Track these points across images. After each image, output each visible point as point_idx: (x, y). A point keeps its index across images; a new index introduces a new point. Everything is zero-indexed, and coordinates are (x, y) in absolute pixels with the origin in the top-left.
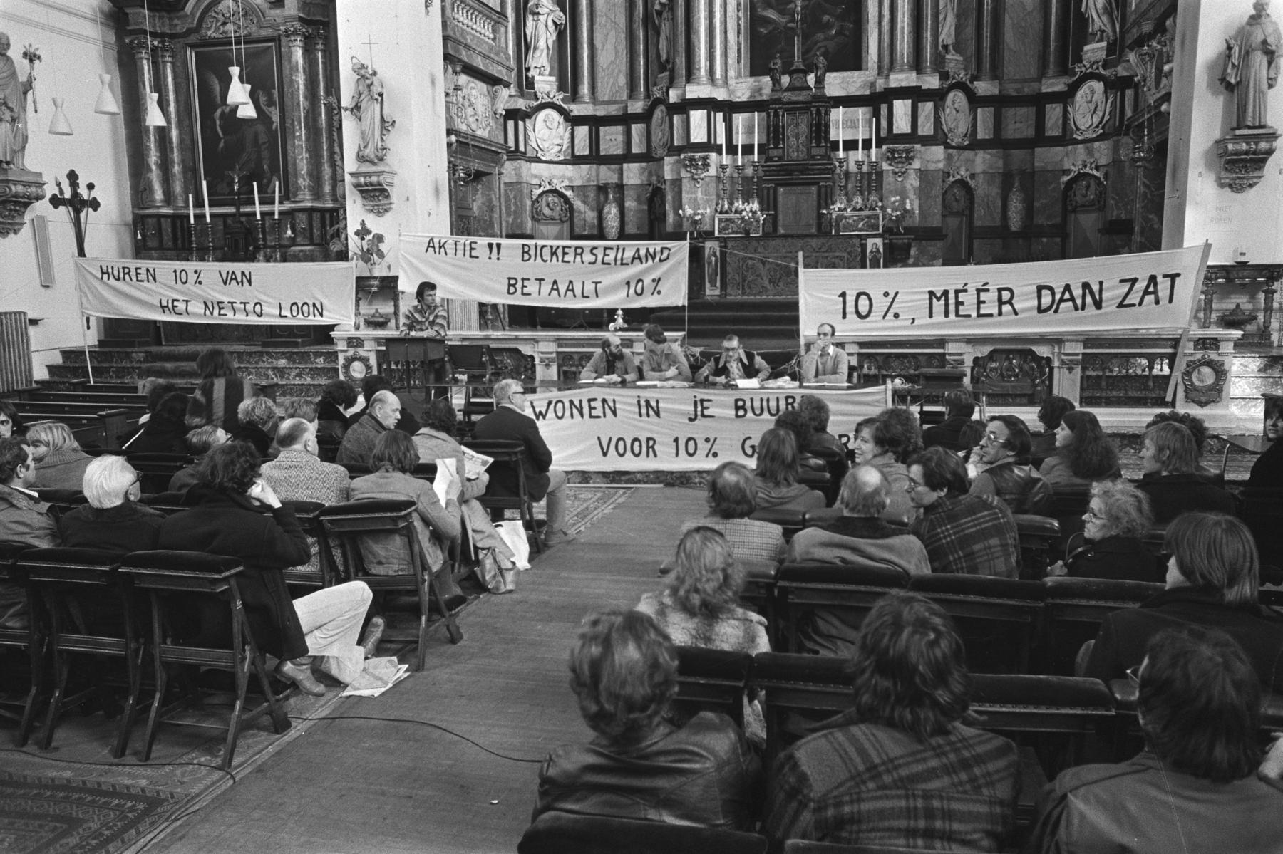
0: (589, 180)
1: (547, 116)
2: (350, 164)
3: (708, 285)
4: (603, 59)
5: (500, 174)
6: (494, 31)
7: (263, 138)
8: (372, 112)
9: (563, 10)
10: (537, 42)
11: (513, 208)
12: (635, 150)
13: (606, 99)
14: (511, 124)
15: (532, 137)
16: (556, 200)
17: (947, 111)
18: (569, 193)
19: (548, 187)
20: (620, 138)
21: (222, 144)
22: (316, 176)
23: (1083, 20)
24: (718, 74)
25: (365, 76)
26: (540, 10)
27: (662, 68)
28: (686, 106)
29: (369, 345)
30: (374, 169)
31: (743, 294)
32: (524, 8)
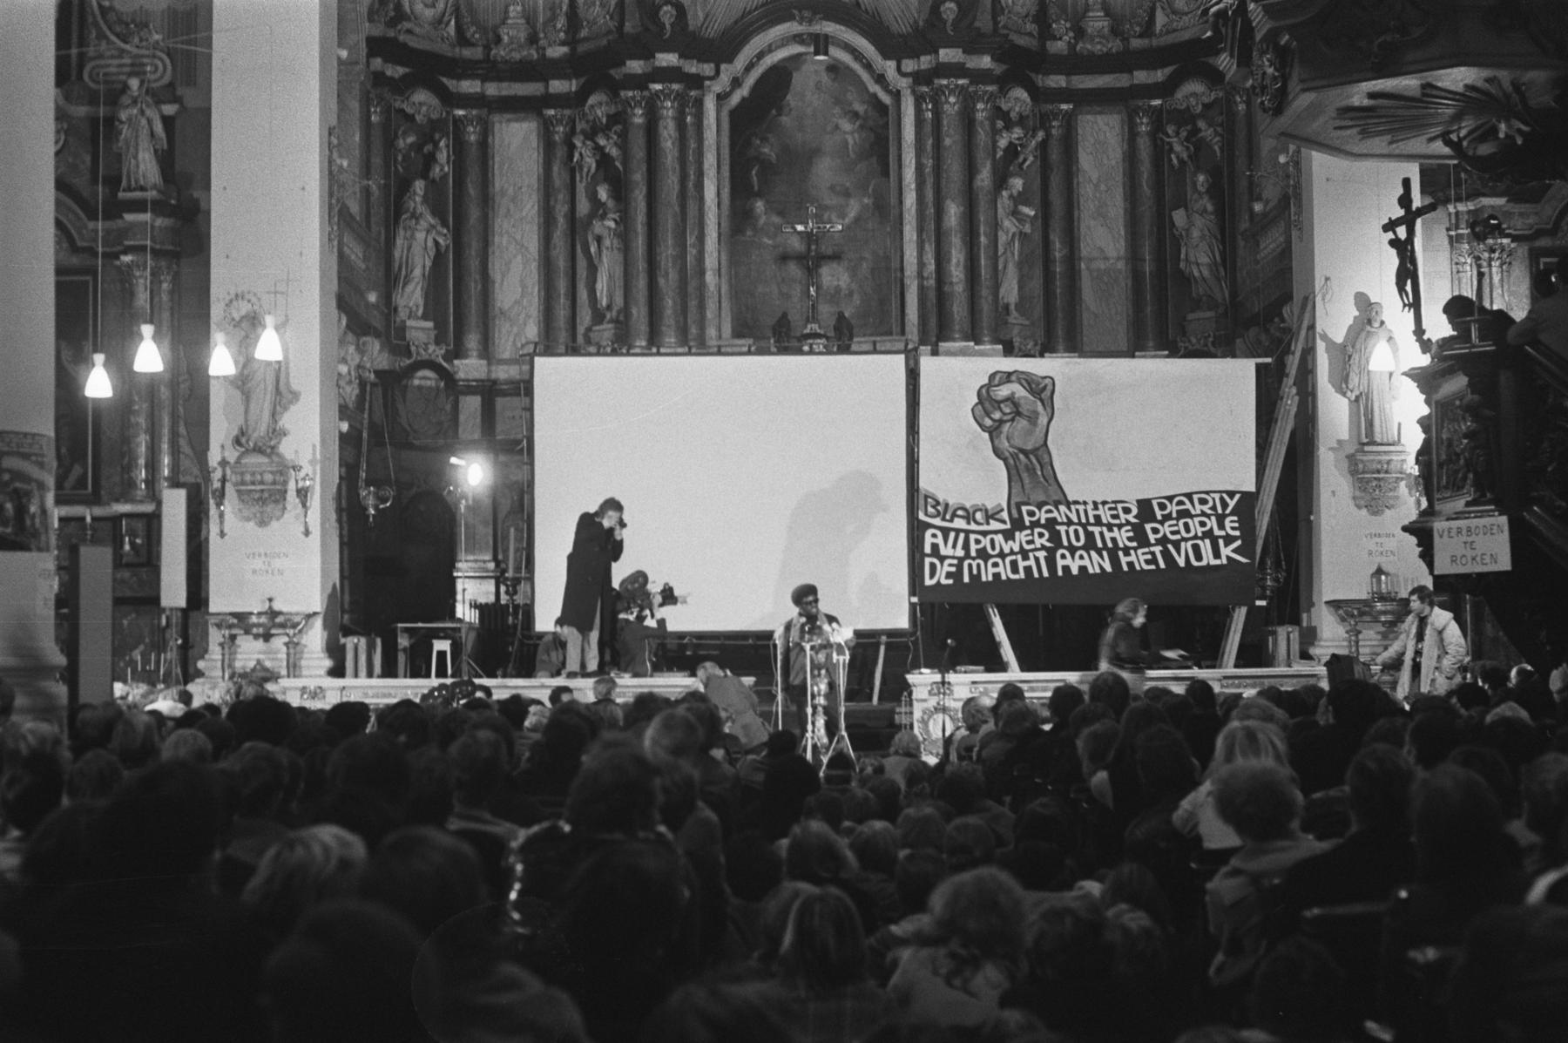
9: (445, 224)
24: (694, 330)
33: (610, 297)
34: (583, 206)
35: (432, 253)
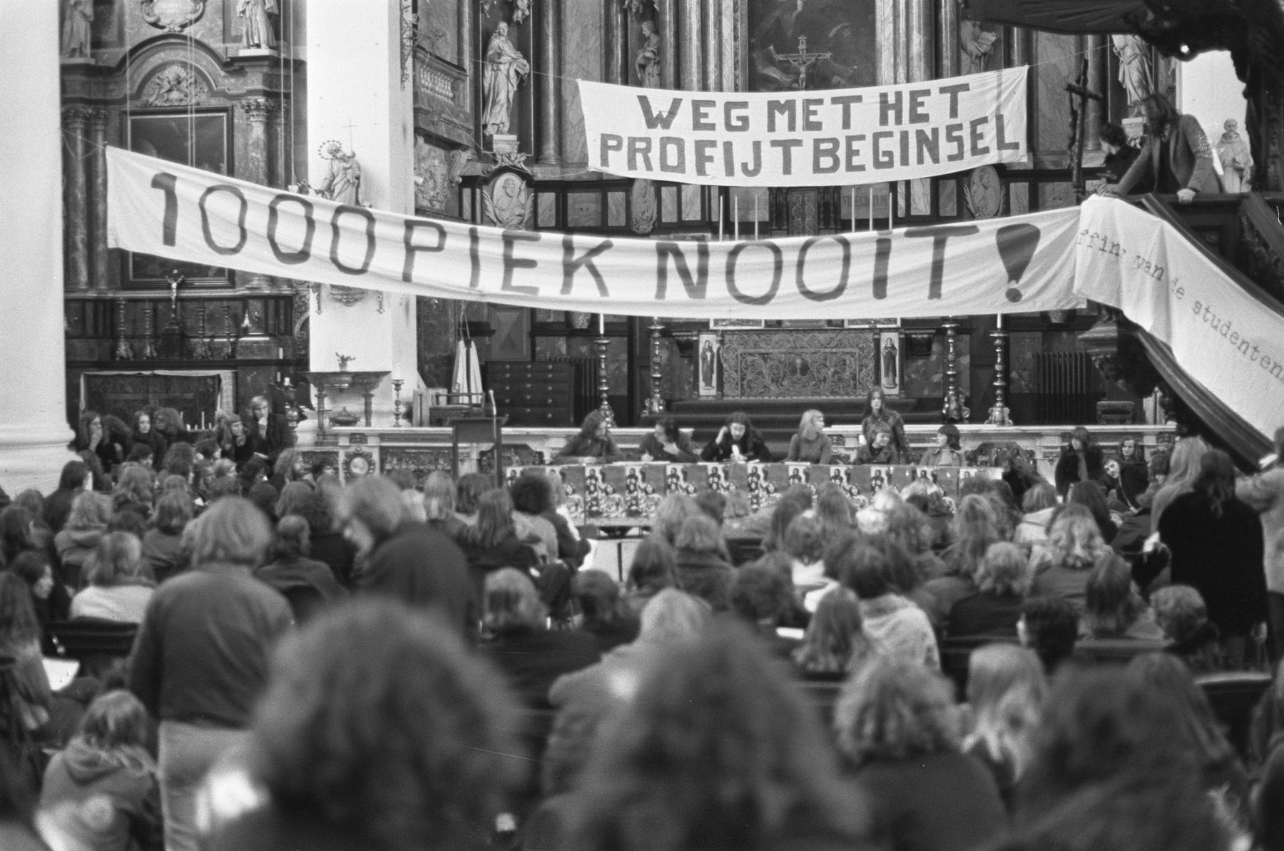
3: (702, 384)
9: (526, 57)
10: (496, 95)
14: (467, 192)
15: (490, 208)
17: (974, 188)
23: (1121, 91)
29: (373, 442)
31: (743, 394)
34: (632, 40)
35: (514, 80)
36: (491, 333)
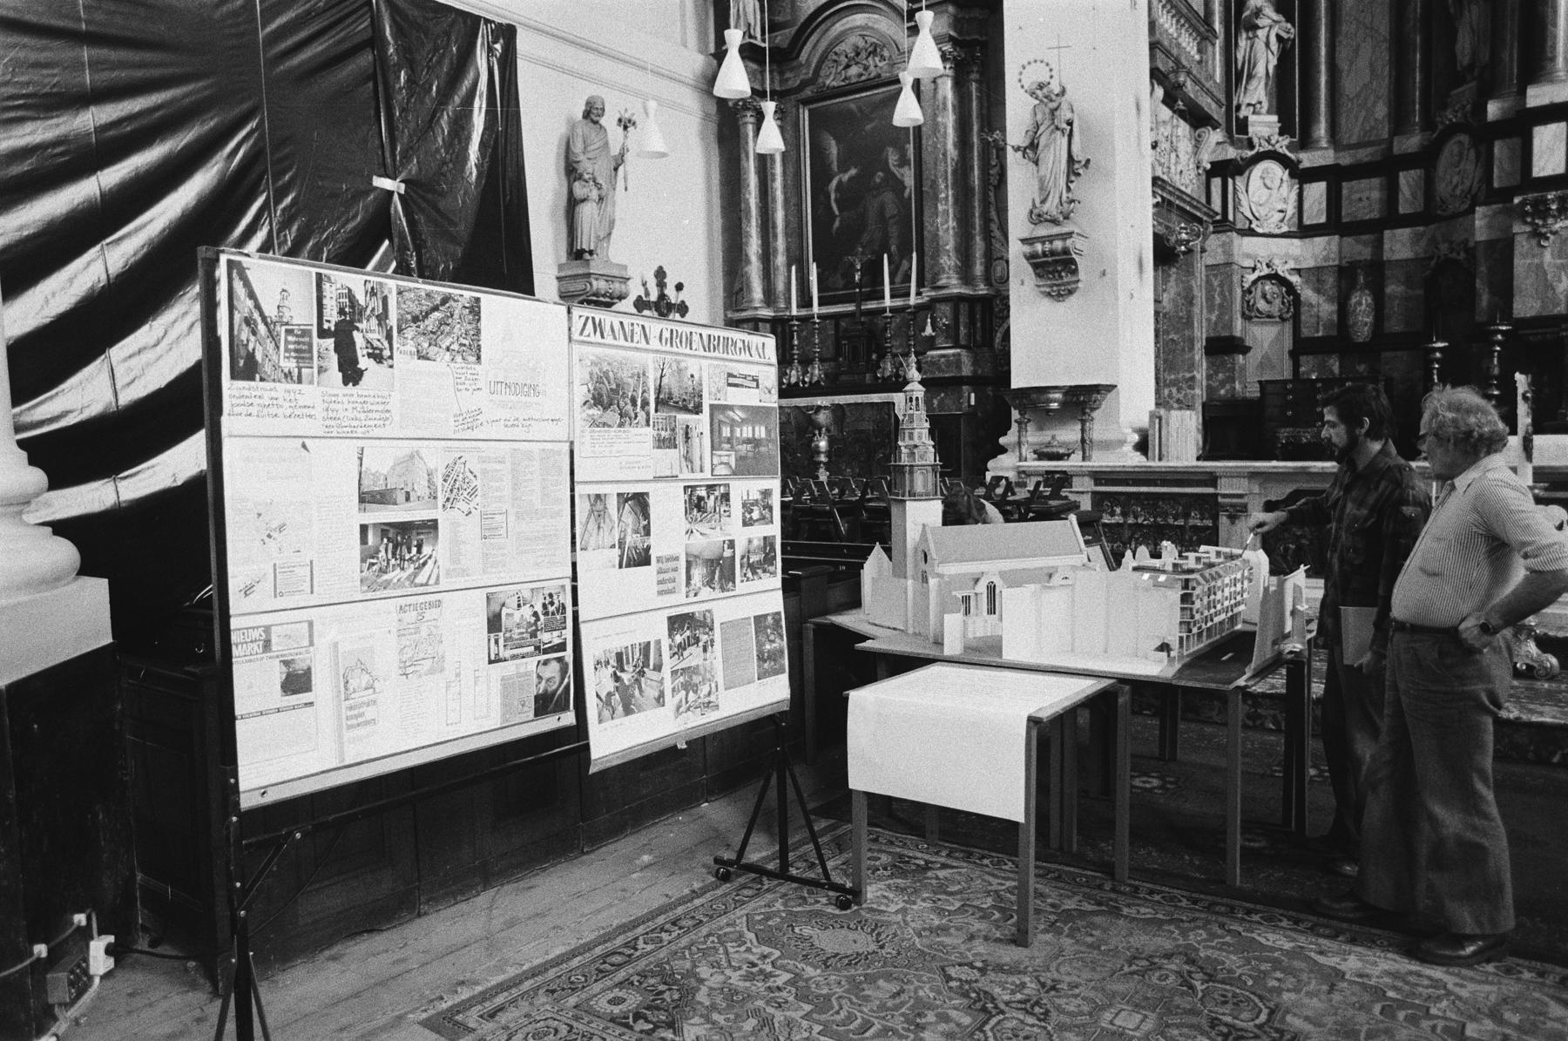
0: (1326, 259)
1: (1266, 171)
2: (1018, 224)
4: (1349, 86)
5: (1203, 250)
6: (1200, 51)
7: (891, 210)
8: (1055, 153)
9: (1290, 19)
11: (1218, 300)
12: (1403, 209)
13: (1354, 140)
14: (1216, 183)
15: (1244, 202)
16: (1276, 289)
18: (1295, 279)
19: (1266, 271)
20: (1376, 195)
21: (837, 224)
22: (965, 252)
25: (1048, 99)
26: (1260, 22)
27: (1459, 80)
28: (1523, 123)
30: (1056, 230)
32: (1240, 20)
33: (1474, 53)
36: (1245, 350)
